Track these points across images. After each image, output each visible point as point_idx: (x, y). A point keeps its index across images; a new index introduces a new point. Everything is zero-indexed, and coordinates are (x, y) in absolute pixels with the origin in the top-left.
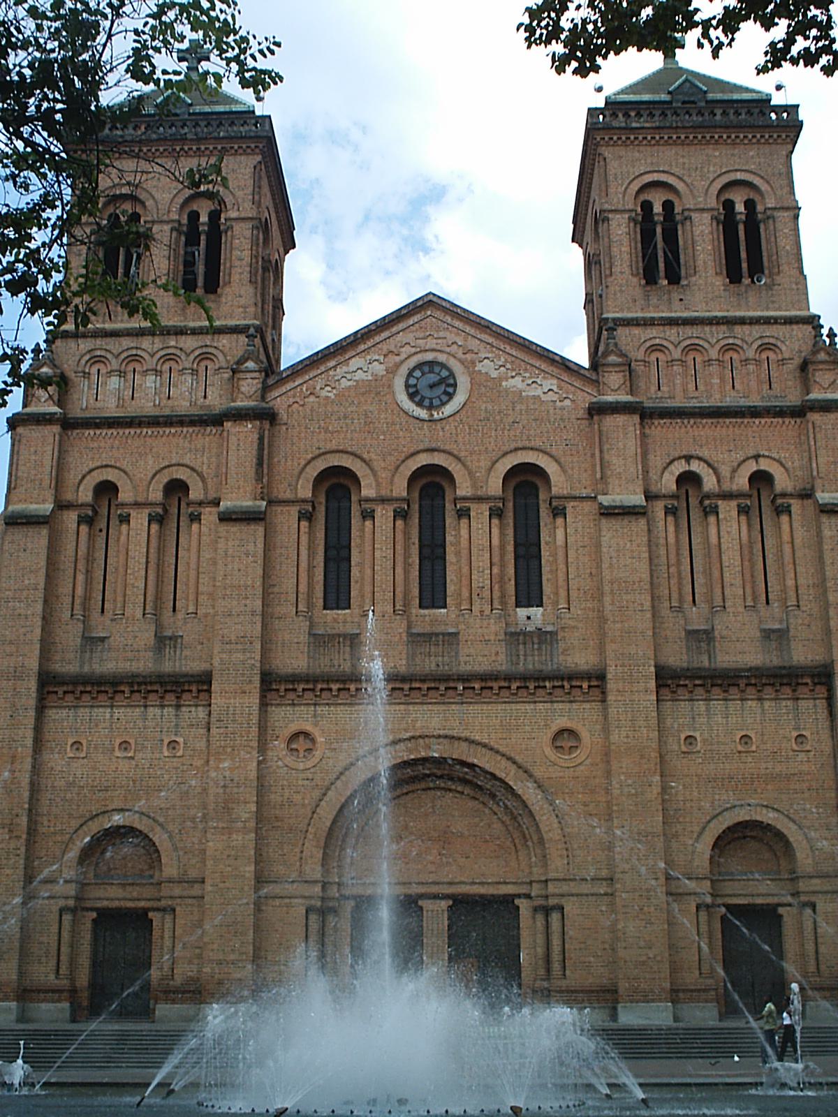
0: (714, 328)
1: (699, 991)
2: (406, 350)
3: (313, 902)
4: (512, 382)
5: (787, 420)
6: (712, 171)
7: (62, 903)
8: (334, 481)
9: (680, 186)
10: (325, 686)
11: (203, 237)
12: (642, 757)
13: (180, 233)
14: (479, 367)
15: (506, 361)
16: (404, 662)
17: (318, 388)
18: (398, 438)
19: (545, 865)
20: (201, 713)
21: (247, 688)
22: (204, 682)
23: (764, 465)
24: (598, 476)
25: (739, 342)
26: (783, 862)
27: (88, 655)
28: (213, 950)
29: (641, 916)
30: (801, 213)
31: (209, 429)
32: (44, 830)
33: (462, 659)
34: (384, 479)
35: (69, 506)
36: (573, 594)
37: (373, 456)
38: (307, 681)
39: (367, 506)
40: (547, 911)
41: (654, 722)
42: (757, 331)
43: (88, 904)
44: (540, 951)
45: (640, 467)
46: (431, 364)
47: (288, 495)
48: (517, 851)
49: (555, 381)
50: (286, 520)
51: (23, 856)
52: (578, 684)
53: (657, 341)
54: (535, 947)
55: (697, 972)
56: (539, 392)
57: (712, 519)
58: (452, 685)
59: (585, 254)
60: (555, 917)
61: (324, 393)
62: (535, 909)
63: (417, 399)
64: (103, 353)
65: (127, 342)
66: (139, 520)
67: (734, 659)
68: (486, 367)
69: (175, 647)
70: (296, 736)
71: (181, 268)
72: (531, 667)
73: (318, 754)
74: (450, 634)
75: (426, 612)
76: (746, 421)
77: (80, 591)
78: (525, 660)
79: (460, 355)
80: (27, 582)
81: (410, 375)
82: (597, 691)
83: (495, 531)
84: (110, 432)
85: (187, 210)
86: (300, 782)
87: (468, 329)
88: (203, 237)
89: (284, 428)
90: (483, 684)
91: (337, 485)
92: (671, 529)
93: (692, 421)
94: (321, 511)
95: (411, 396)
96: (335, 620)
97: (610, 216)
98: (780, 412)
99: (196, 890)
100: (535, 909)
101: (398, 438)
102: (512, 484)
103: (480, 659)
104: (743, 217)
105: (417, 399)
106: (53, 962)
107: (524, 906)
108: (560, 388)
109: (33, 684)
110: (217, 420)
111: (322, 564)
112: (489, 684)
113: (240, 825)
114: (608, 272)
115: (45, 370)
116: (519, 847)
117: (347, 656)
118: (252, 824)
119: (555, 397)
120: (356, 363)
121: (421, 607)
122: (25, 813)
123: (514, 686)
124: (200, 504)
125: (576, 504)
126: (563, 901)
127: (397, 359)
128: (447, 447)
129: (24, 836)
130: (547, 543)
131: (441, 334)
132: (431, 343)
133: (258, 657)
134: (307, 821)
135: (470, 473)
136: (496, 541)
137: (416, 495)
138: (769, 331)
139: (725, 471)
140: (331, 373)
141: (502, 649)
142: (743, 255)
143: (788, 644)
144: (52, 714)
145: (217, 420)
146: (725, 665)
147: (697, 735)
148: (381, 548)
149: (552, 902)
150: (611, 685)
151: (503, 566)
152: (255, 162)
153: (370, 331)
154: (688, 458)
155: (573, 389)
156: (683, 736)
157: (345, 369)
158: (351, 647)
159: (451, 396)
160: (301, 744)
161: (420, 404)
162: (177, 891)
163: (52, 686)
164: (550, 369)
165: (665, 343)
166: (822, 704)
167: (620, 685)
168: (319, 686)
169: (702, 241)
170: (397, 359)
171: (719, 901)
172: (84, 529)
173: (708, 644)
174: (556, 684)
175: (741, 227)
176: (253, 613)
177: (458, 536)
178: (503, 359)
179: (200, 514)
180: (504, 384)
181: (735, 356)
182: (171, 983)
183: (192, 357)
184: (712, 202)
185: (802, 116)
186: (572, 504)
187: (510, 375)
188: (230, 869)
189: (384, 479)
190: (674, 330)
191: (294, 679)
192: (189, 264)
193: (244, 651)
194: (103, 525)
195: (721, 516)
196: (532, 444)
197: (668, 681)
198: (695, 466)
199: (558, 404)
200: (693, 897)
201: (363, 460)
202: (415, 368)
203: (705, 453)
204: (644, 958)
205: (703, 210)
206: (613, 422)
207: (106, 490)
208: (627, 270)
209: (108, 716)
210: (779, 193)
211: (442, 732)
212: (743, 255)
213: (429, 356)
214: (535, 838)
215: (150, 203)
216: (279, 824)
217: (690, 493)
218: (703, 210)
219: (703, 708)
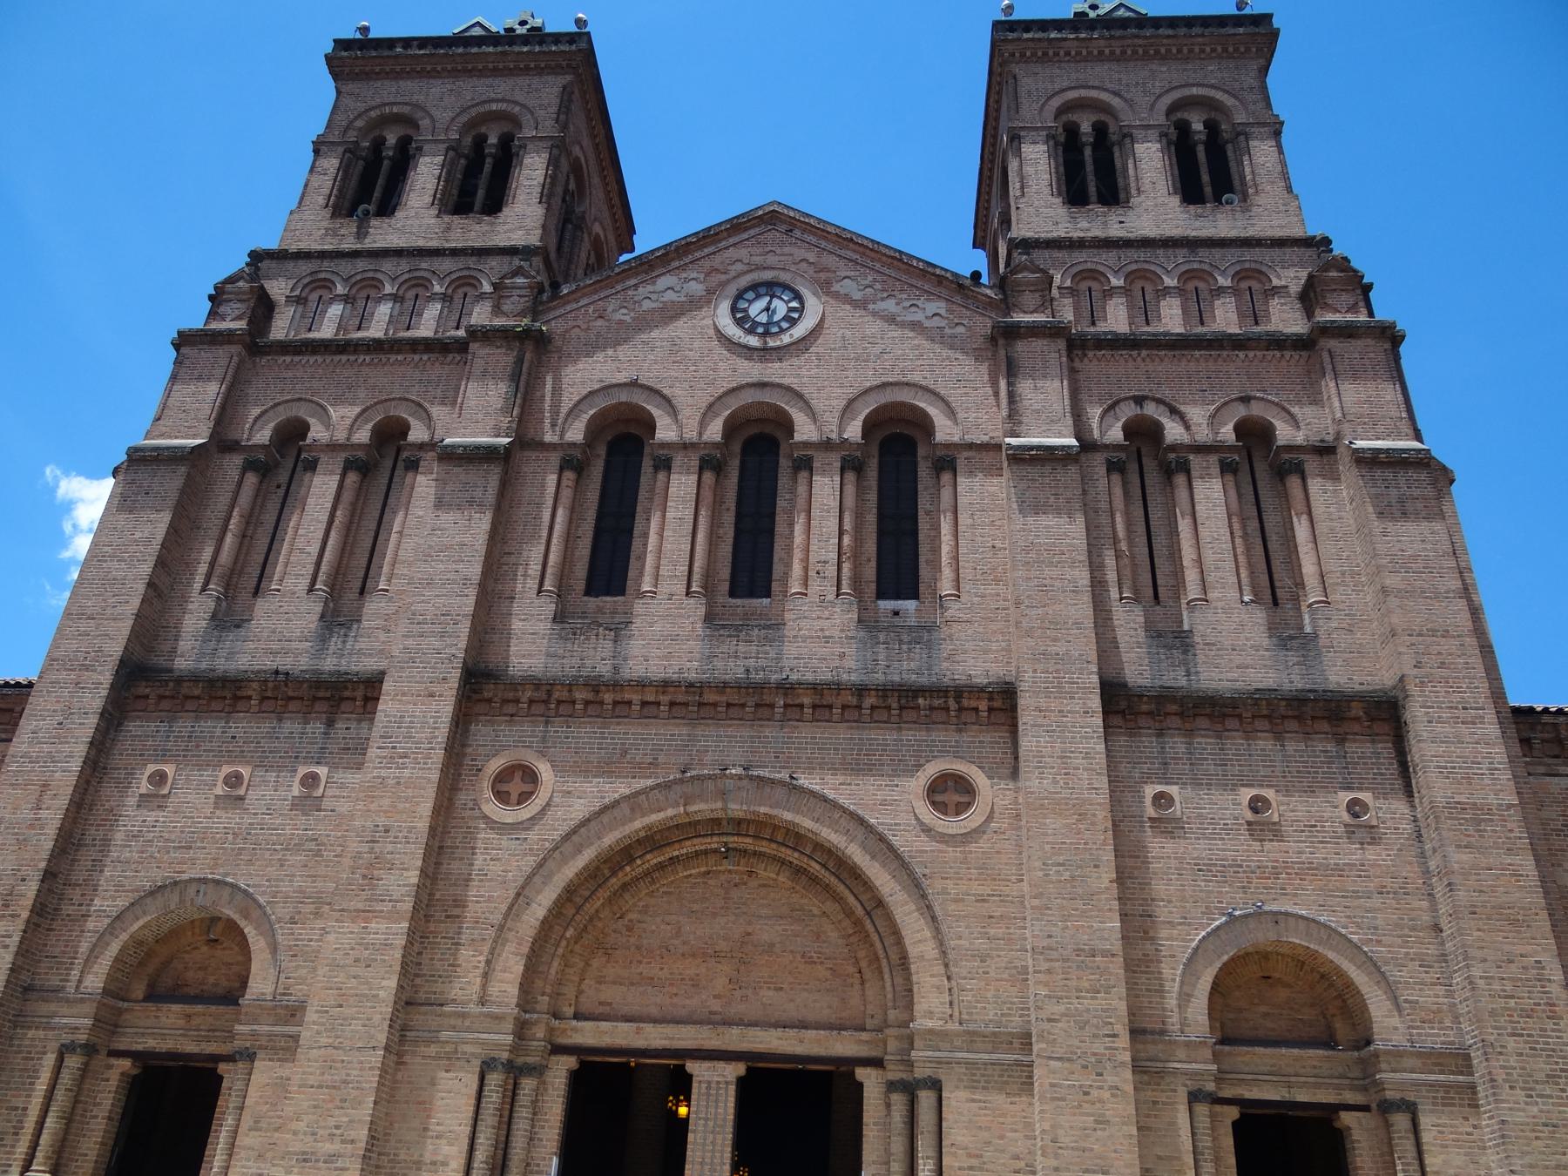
0: (1170, 251)
2: (739, 267)
3: (495, 1054)
4: (881, 305)
5: (1287, 354)
6: (1158, 86)
7: (66, 1038)
9: (1115, 102)
12: (1082, 816)
13: (459, 155)
15: (875, 280)
17: (610, 309)
19: (910, 1006)
21: (436, 688)
23: (1256, 410)
25: (1206, 267)
27: (213, 644)
28: (295, 1133)
29: (1087, 1108)
30: (1285, 129)
32: (71, 910)
35: (232, 447)
36: (966, 573)
40: (909, 1089)
42: (1232, 255)
43: (123, 1044)
45: (1067, 402)
47: (549, 437)
48: (863, 983)
49: (943, 304)
51: (13, 949)
52: (973, 704)
53: (1089, 266)
54: (887, 1163)
56: (919, 316)
57: (1180, 480)
59: (988, 256)
60: (926, 1098)
61: (617, 316)
62: (892, 1086)
64: (328, 276)
67: (1230, 675)
71: (455, 192)
72: (896, 678)
75: (739, 601)
76: (1225, 353)
80: (138, 535)
82: (1001, 718)
83: (850, 489)
84: (312, 360)
87: (823, 244)
92: (1118, 491)
93: (1144, 353)
95: (739, 322)
98: (1278, 342)
100: (892, 1086)
102: (879, 436)
104: (1203, 137)
106: (22, 1149)
107: (871, 1081)
108: (950, 311)
109: (105, 677)
111: (590, 534)
114: (1018, 193)
116: (867, 974)
118: (408, 906)
119: (943, 323)
120: (664, 282)
121: (732, 594)
122: (38, 875)
124: (422, 446)
125: (971, 454)
127: (723, 277)
128: (786, 381)
129: (25, 915)
130: (928, 513)
133: (463, 644)
137: (737, 448)
138: (1248, 255)
141: (851, 650)
142: (1206, 178)
143: (1319, 655)
144: (134, 727)
146: (1214, 685)
149: (919, 1073)
150: (1025, 718)
152: (564, 82)
153: (688, 244)
154: (1139, 400)
157: (650, 288)
160: (515, 787)
161: (751, 331)
163: (144, 686)
164: (936, 290)
165: (1101, 268)
166: (1385, 749)
167: (1043, 702)
169: (1149, 163)
170: (723, 277)
171: (1227, 1093)
172: (251, 479)
173: (1185, 652)
174: (936, 703)
175: (1201, 149)
177: (793, 491)
178: (870, 278)
179: (418, 460)
181: (1201, 285)
183: (448, 280)
184: (1162, 120)
185: (1276, 23)
186: (966, 454)
190: (1113, 254)
193: (442, 635)
194: (283, 478)
195: (1194, 473)
197: (1121, 704)
198: (1151, 409)
199: (947, 331)
201: (664, 397)
202: (746, 290)
203: (1165, 393)
205: (1148, 127)
208: (1047, 191)
209: (218, 731)
210: (1252, 107)
212: (1206, 178)
213: (768, 275)
214: (894, 957)
215: (425, 123)
216: (456, 911)
217: (1144, 451)
218: (1148, 127)
219: (1182, 748)
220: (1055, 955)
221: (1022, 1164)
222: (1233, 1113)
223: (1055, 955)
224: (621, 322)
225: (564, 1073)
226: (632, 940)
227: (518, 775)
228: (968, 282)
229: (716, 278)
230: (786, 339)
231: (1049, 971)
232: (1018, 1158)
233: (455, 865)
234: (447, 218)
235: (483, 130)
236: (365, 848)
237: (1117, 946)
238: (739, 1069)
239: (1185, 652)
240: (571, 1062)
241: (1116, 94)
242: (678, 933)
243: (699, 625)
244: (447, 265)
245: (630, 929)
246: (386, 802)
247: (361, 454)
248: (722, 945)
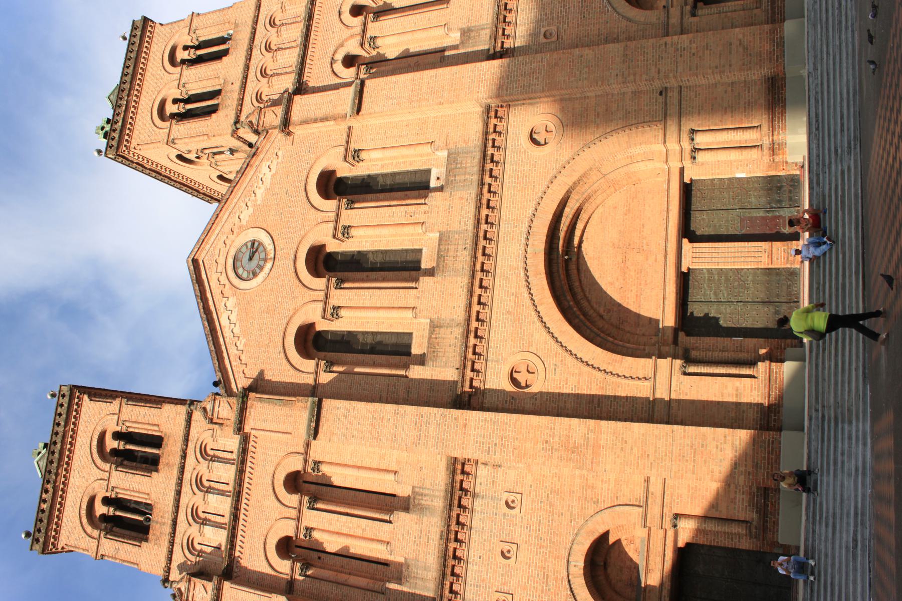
1: (773, 8)
8: (310, 343)
10: (471, 350)
12: (556, 65)
14: (244, 222)
16: (459, 279)
18: (283, 286)
21: (461, 422)
22: (459, 469)
24: (332, 123)
31: (251, 448)
33: (463, 228)
37: (292, 307)
38: (464, 367)
39: (329, 311)
40: (695, 150)
41: (527, 58)
44: (734, 155)
55: (756, 11)
58: (481, 234)
63: (258, 270)
65: (181, 517)
66: (311, 518)
68: (246, 215)
69: (422, 495)
71: (144, 466)
74: (440, 240)
77: (362, 582)
78: (469, 174)
79: (231, 237)
85: (109, 457)
86: (557, 377)
88: (129, 447)
89: (259, 382)
90: (484, 206)
91: (310, 341)
95: (255, 275)
97: (172, 137)
99: (656, 488)
101: (283, 286)
103: (464, 212)
105: (258, 270)
108: (268, 160)
112: (484, 201)
113: (591, 435)
115: (183, 590)
117: (449, 330)
118: (591, 422)
119: (275, 162)
120: (224, 321)
123: (487, 180)
124: (306, 460)
131: (217, 252)
132: (221, 260)
134: (595, 372)
139: (348, 33)
140: (227, 340)
141: (458, 194)
147: (543, 30)
154: (333, 61)
155: (271, 150)
156: (544, 40)
158: (440, 327)
159: (260, 244)
161: (261, 268)
162: (654, 510)
168: (470, 355)
170: (228, 285)
173: (472, 31)
176: (396, 413)
180: (259, 203)
182: (754, 523)
187: (253, 198)
188: (635, 450)
194: (315, 555)
196: (304, 178)
198: (340, 56)
199: (279, 160)
200: (685, 20)
204: (741, 50)
206: (295, 116)
207: (286, 547)
209: (476, 568)
211: (523, 242)
213: (230, 262)
220: (626, 73)
221: (730, 89)
223: (626, 73)
224: (245, 345)
225: (688, 338)
226: (615, 309)
228: (254, 150)
229: (228, 290)
230: (270, 247)
231: (635, 75)
232: (726, 92)
233: (569, 405)
234: (161, 466)
236: (556, 454)
237: (623, 44)
238: (685, 241)
239: (472, 31)
240: (681, 335)
241: (159, 92)
243: (435, 279)
244: (190, 461)
245: (609, 311)
246: (528, 445)
247: (306, 498)
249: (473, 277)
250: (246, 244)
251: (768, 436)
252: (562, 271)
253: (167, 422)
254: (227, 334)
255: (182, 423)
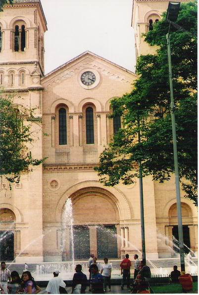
11: (20, 34)
20: (27, 175)
26: (189, 213)
34: (75, 108)
40: (123, 228)
46: (88, 72)
47: (48, 112)
50: (48, 119)
68: (106, 73)
70: (53, 181)
73: (59, 186)
75: (88, 145)
81: (82, 75)
83: (108, 121)
88: (20, 34)
91: (62, 109)
94: (58, 116)
96: (62, 148)
110: (26, 91)
117: (66, 159)
120: (66, 72)
121: (87, 143)
126: (128, 226)
135: (101, 104)
136: (108, 124)
137: (85, 111)
145: (26, 91)
148: (75, 127)
151: (110, 131)
157: (63, 74)
158: (67, 155)
160: (54, 184)
161: (85, 84)
168: (59, 167)
180: (109, 77)
189: (75, 108)
191: (52, 165)
192: (16, 41)
199: (125, 83)
222: (173, 227)
227: (54, 182)
233: (47, 199)
234: (15, 52)
235: (17, 24)
242: (84, 206)
244: (18, 67)
248: (92, 208)
249: (82, 165)
250: (94, 75)
251: (42, 253)
252: (86, 191)
253: (30, 53)
254: (62, 75)
255: (30, 60)
